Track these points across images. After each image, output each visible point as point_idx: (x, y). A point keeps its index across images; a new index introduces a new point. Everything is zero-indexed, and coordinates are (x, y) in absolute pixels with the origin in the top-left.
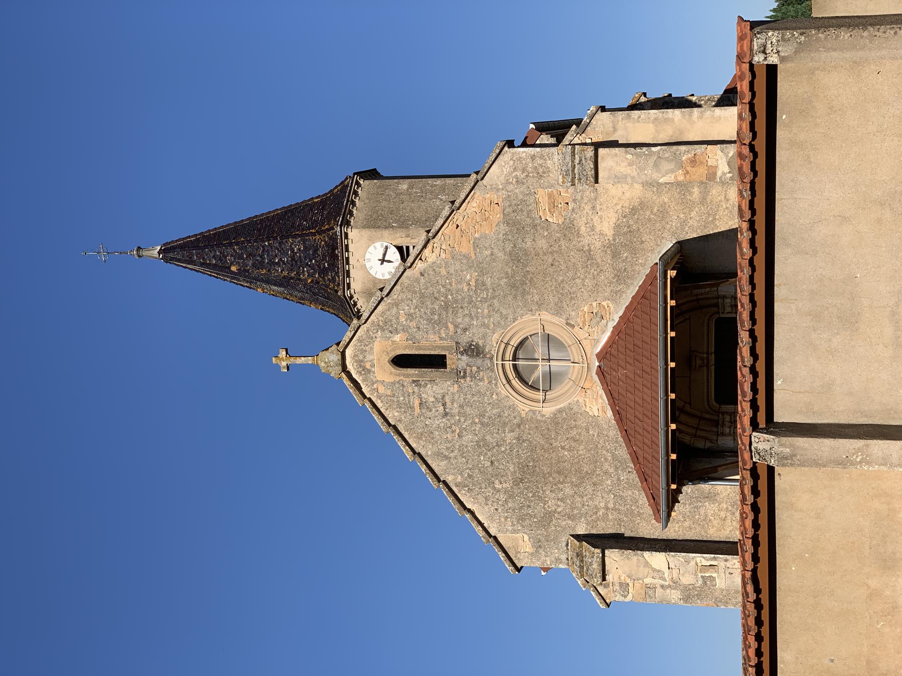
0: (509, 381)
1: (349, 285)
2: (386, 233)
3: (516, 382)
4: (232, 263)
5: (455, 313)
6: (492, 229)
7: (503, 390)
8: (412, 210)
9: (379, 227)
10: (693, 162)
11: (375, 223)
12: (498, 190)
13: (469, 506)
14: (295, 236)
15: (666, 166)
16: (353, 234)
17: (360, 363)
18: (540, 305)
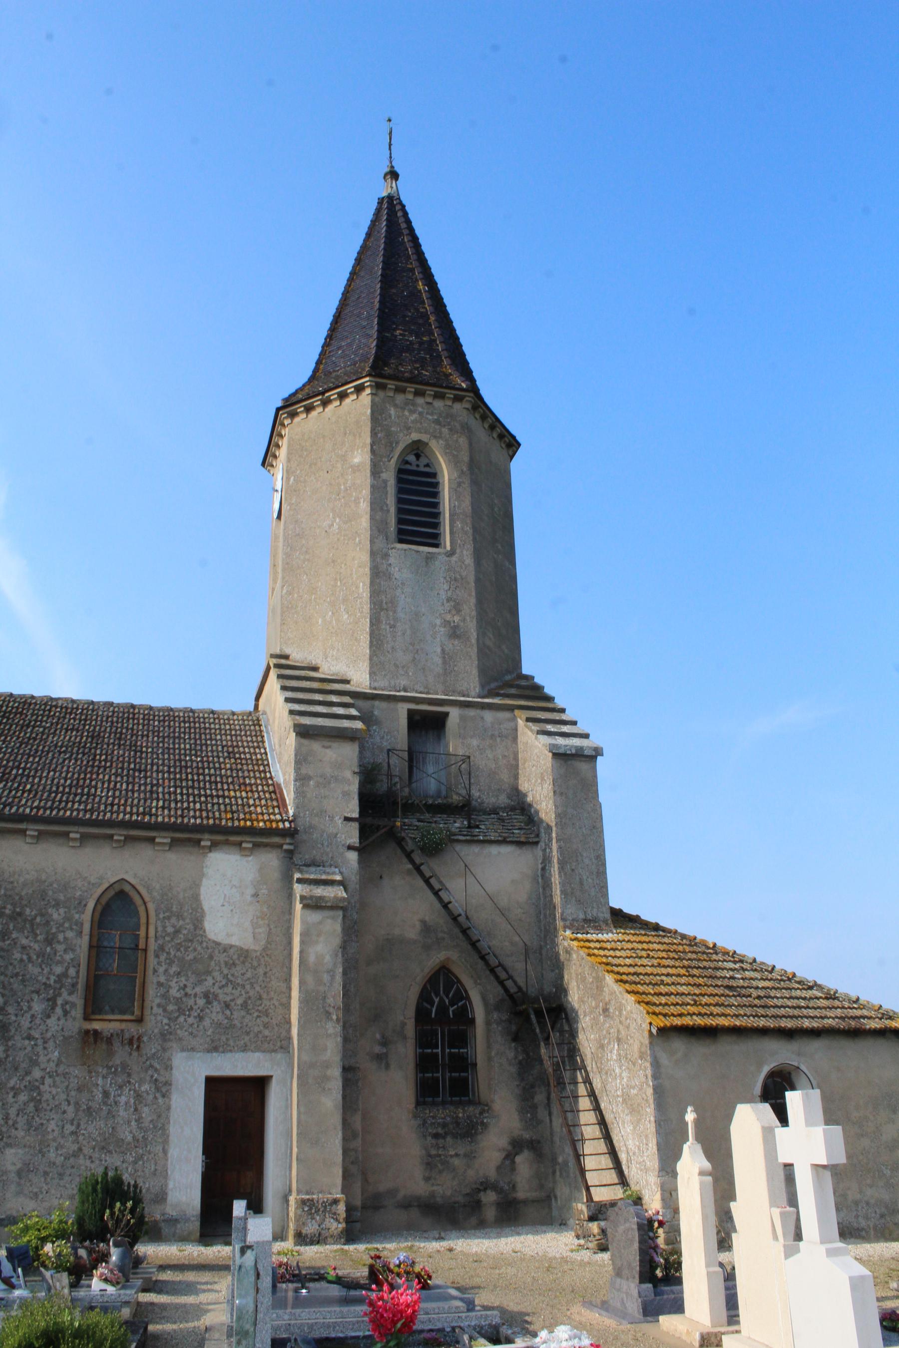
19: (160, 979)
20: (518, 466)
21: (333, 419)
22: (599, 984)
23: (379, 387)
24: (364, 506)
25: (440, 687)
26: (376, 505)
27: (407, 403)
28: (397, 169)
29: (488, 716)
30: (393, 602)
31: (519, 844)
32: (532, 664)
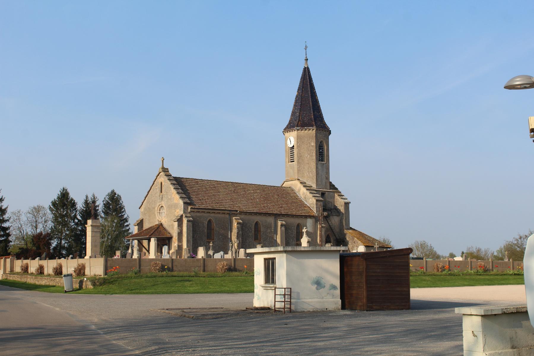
7: (158, 204)
11: (299, 139)
14: (300, 113)
20: (330, 137)
22: (353, 239)
23: (317, 130)
24: (314, 154)
28: (308, 58)
29: (331, 193)
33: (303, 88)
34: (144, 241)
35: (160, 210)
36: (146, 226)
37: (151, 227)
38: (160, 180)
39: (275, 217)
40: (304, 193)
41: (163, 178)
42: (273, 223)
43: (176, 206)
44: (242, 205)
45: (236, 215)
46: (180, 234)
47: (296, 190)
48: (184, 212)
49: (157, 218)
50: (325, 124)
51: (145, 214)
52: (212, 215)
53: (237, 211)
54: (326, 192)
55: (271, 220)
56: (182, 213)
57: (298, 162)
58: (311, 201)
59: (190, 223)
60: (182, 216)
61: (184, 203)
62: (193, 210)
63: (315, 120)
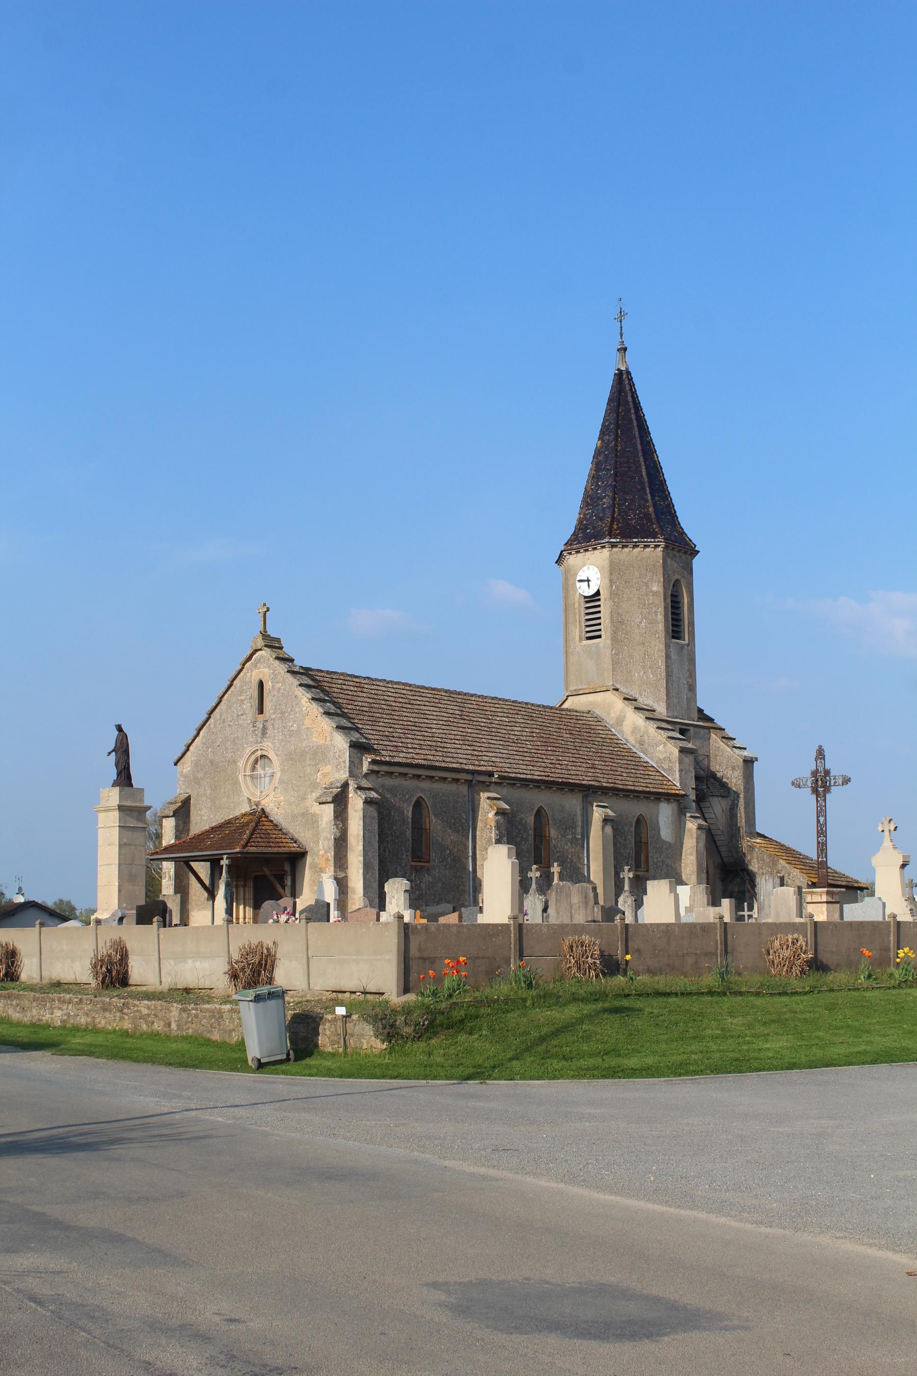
0: (253, 753)
1: (570, 554)
2: (607, 581)
3: (253, 757)
4: (603, 441)
5: (280, 718)
6: (316, 740)
7: (248, 750)
8: (629, 599)
9: (611, 574)
10: (327, 860)
11: (614, 571)
12: (331, 741)
13: (201, 733)
15: (326, 843)
16: (606, 552)
17: (258, 661)
18: (282, 770)
19: (654, 857)
21: (639, 558)
23: (666, 547)
24: (660, 617)
25: (686, 717)
26: (666, 617)
27: (674, 556)
28: (626, 345)
29: (702, 731)
30: (672, 671)
31: (723, 797)
32: (704, 702)
33: (618, 426)
34: (164, 863)
35: (254, 768)
36: (203, 819)
37: (228, 822)
38: (252, 674)
39: (585, 797)
40: (635, 730)
41: (266, 668)
42: (579, 813)
43: (319, 755)
44: (497, 759)
45: (486, 786)
46: (341, 843)
47: (610, 719)
48: (352, 774)
49: (246, 794)
50: (683, 533)
51: (197, 781)
52: (426, 785)
53: (491, 774)
54: (692, 726)
55: (573, 803)
56: (343, 775)
57: (614, 639)
58: (663, 755)
59: (373, 811)
60: (345, 785)
61: (354, 745)
62: (375, 768)
63: (657, 518)
